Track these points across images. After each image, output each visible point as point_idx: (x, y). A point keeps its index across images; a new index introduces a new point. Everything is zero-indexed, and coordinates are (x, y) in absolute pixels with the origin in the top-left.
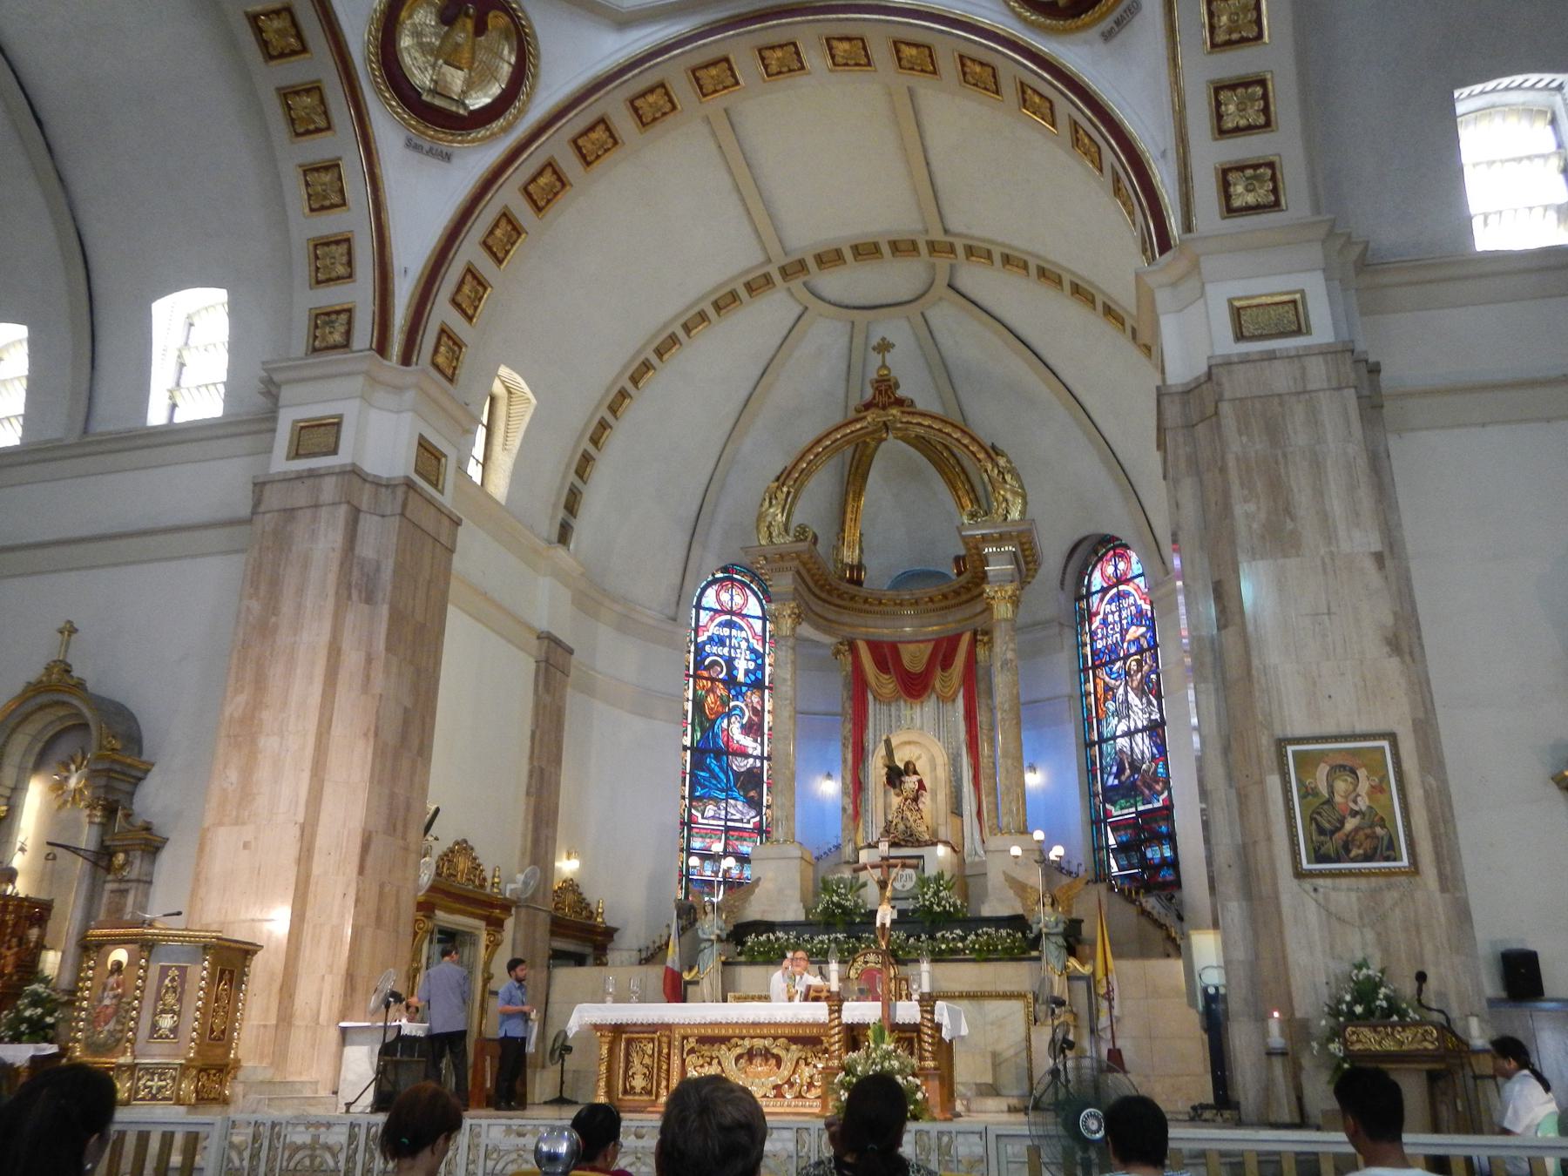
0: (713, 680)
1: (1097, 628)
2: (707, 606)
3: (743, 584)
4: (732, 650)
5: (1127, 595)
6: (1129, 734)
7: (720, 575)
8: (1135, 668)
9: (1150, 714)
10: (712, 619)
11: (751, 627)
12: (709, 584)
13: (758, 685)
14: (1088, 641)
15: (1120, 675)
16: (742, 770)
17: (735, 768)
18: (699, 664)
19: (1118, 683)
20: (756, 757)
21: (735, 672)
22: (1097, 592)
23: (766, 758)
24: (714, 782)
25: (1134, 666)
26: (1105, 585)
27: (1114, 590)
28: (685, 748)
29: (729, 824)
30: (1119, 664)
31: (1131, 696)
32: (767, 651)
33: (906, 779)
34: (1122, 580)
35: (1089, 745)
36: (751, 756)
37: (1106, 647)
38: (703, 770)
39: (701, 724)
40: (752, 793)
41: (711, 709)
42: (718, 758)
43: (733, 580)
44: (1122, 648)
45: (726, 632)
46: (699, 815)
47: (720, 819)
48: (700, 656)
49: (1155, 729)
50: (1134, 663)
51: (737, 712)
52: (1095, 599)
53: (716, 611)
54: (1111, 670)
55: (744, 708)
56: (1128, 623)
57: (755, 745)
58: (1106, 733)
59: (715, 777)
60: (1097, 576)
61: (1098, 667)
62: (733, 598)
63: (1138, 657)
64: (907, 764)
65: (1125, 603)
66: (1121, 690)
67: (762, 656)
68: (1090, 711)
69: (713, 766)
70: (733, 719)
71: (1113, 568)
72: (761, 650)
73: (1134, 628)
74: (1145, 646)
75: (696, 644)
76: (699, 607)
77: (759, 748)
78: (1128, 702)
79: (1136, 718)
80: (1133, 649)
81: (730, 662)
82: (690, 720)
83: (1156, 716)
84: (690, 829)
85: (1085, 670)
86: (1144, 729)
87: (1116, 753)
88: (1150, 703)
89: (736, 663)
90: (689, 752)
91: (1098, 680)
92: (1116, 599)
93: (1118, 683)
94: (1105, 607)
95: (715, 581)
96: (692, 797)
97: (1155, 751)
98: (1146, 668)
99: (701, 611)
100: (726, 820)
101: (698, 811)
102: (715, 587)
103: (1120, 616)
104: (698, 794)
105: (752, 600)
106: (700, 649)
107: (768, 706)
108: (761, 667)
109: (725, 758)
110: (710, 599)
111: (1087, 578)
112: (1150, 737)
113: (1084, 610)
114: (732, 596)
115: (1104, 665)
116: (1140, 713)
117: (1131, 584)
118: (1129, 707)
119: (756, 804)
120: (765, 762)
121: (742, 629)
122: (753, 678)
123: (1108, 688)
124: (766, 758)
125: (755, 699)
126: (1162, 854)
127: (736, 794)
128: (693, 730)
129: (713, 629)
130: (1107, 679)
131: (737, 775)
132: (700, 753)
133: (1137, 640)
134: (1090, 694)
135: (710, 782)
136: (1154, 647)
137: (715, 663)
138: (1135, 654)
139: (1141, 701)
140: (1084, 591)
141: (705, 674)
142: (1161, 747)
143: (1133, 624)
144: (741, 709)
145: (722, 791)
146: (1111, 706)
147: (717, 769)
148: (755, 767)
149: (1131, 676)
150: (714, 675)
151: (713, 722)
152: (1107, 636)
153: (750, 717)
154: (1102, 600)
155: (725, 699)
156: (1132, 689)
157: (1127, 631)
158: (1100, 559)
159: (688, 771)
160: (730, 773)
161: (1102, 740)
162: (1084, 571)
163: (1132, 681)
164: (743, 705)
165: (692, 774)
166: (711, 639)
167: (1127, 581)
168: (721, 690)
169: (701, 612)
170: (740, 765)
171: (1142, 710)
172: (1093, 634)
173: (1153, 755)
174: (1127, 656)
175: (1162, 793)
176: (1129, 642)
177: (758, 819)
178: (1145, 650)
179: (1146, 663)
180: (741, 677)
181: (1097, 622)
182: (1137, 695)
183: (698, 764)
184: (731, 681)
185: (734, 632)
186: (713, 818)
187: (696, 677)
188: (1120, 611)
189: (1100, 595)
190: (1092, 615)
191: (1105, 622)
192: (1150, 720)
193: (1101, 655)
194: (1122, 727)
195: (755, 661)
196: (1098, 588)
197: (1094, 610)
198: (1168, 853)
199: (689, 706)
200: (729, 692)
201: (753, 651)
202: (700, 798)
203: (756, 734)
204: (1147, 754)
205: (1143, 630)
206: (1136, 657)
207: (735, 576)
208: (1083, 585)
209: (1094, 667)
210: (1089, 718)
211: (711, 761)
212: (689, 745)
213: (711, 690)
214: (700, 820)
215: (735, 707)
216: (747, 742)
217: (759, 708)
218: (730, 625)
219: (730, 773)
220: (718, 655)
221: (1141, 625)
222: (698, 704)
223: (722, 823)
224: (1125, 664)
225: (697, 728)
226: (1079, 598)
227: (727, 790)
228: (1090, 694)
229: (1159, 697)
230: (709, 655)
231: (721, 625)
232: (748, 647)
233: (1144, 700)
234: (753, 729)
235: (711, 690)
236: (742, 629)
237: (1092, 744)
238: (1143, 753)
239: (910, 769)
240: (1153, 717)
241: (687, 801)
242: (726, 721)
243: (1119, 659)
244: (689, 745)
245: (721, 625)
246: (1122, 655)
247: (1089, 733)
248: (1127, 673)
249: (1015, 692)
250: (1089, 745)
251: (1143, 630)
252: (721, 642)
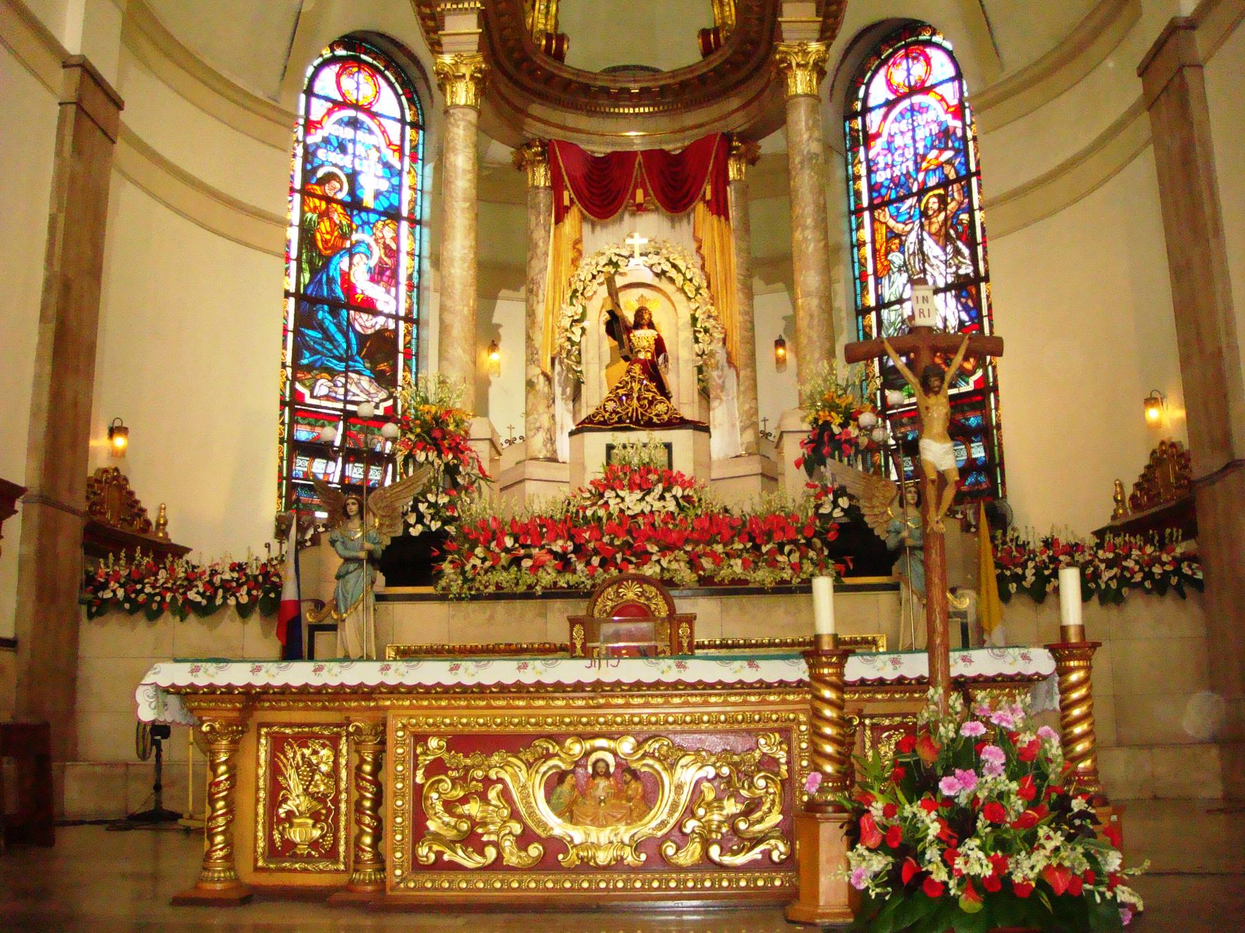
0: (329, 200)
1: (878, 154)
2: (322, 93)
3: (375, 71)
4: (357, 160)
5: (922, 110)
7: (340, 52)
8: (936, 206)
9: (958, 268)
10: (329, 113)
11: (384, 132)
12: (326, 63)
13: (392, 214)
14: (862, 169)
15: (910, 218)
16: (369, 332)
17: (358, 328)
18: (307, 175)
19: (908, 228)
20: (389, 316)
21: (359, 193)
22: (880, 106)
23: (402, 318)
24: (330, 347)
25: (934, 204)
26: (892, 97)
27: (905, 104)
28: (287, 294)
29: (350, 407)
30: (912, 201)
31: (931, 247)
32: (406, 168)
33: (638, 333)
34: (922, 88)
36: (380, 313)
37: (892, 180)
38: (313, 329)
39: (310, 262)
40: (383, 366)
41: (325, 242)
42: (334, 312)
43: (361, 64)
44: (916, 179)
45: (348, 133)
46: (306, 392)
47: (336, 400)
48: (311, 163)
49: (965, 288)
50: (935, 200)
51: (362, 248)
52: (874, 119)
53: (335, 102)
54: (898, 209)
55: (373, 244)
56: (925, 146)
57: (386, 297)
58: (889, 295)
59: (329, 337)
60: (879, 81)
61: (879, 206)
62: (360, 86)
63: (941, 191)
64: (640, 313)
65: (920, 119)
66: (912, 238)
67: (400, 174)
68: (863, 265)
69: (327, 323)
70: (356, 259)
71: (905, 74)
72: (398, 166)
73: (934, 153)
74: (952, 176)
75: (306, 147)
76: (310, 92)
77: (393, 302)
78: (923, 253)
79: (936, 274)
80: (932, 181)
81: (353, 177)
82: (294, 254)
83: (966, 269)
84: (293, 412)
85: (858, 211)
86: (948, 288)
87: (903, 322)
88: (957, 252)
89: (361, 179)
90: (292, 300)
91: (877, 225)
92: (908, 115)
93: (908, 228)
95: (333, 60)
96: (296, 366)
97: (964, 317)
98: (952, 206)
99: (314, 100)
100: (346, 402)
101: (304, 385)
102: (335, 68)
103: (913, 138)
104: (305, 362)
105: (386, 91)
106: (309, 155)
107: (406, 244)
108: (397, 189)
109: (344, 312)
110: (326, 82)
111: (863, 88)
112: (958, 297)
113: (857, 131)
114: (358, 83)
115: (890, 202)
116: (943, 266)
117: (932, 94)
118: (924, 258)
119: (386, 380)
120: (401, 323)
121: (370, 132)
122: (386, 204)
123: (892, 235)
124: (402, 318)
125: (388, 233)
126: (969, 454)
127: (360, 366)
128: (300, 270)
129: (330, 128)
130: (891, 223)
131: (362, 338)
132: (306, 302)
133: (940, 166)
134: (864, 244)
135: (324, 347)
137: (330, 177)
138: (936, 187)
139: (944, 249)
140: (858, 106)
141: (318, 190)
142: (975, 310)
143: (933, 147)
144: (369, 246)
145: (340, 359)
146: (896, 258)
147: (333, 329)
148: (387, 330)
149: (928, 217)
150: (331, 194)
151: (328, 261)
152: (893, 166)
153: (380, 258)
154: (885, 118)
155: (346, 229)
156: (930, 234)
157: (924, 157)
158: (884, 62)
159: (291, 326)
160: (352, 335)
161: (881, 305)
162: (857, 78)
163: (930, 224)
164: (371, 241)
165: (297, 332)
166: (326, 141)
168: (338, 215)
169: (314, 100)
170: (365, 323)
171: (946, 262)
173: (961, 323)
174: (923, 191)
175: (973, 373)
176: (927, 171)
177: (390, 402)
178: (954, 182)
179: (953, 199)
180: (369, 202)
181: (878, 145)
182: (937, 243)
183: (305, 318)
184: (354, 205)
185: (361, 135)
186: (327, 397)
187: (306, 193)
188: (913, 130)
189: (883, 110)
190: (869, 139)
191: (889, 149)
192: (957, 276)
193: (883, 191)
195: (389, 179)
196: (882, 101)
197: (873, 131)
198: (978, 452)
199: (293, 234)
200: (352, 222)
201: (387, 165)
202: (309, 368)
203: (389, 284)
204: (953, 323)
205: (949, 154)
206: (936, 192)
207: (363, 57)
208: (857, 99)
209: (872, 208)
210: (863, 277)
211: (323, 314)
212: (292, 289)
213: (325, 214)
214: (308, 400)
215: (358, 243)
216: (375, 292)
217: (394, 246)
218: (354, 124)
219: (352, 335)
220: (335, 165)
221: (946, 148)
222: (307, 233)
223: (340, 405)
224: (919, 201)
225: (305, 266)
226: (852, 116)
227: (346, 359)
228: (864, 244)
229: (972, 245)
230: (322, 165)
231: (340, 122)
232: (380, 158)
233: (949, 249)
234: (384, 274)
235: (325, 214)
236: (370, 132)
237: (866, 311)
238: (945, 320)
239: (642, 319)
240: (962, 272)
241: (289, 370)
242: (346, 259)
243: (911, 195)
244: (292, 289)
245: (340, 122)
246: (915, 189)
247: (863, 296)
248: (924, 214)
249: (822, 202)
250: (864, 311)
251: (949, 154)
252: (342, 148)
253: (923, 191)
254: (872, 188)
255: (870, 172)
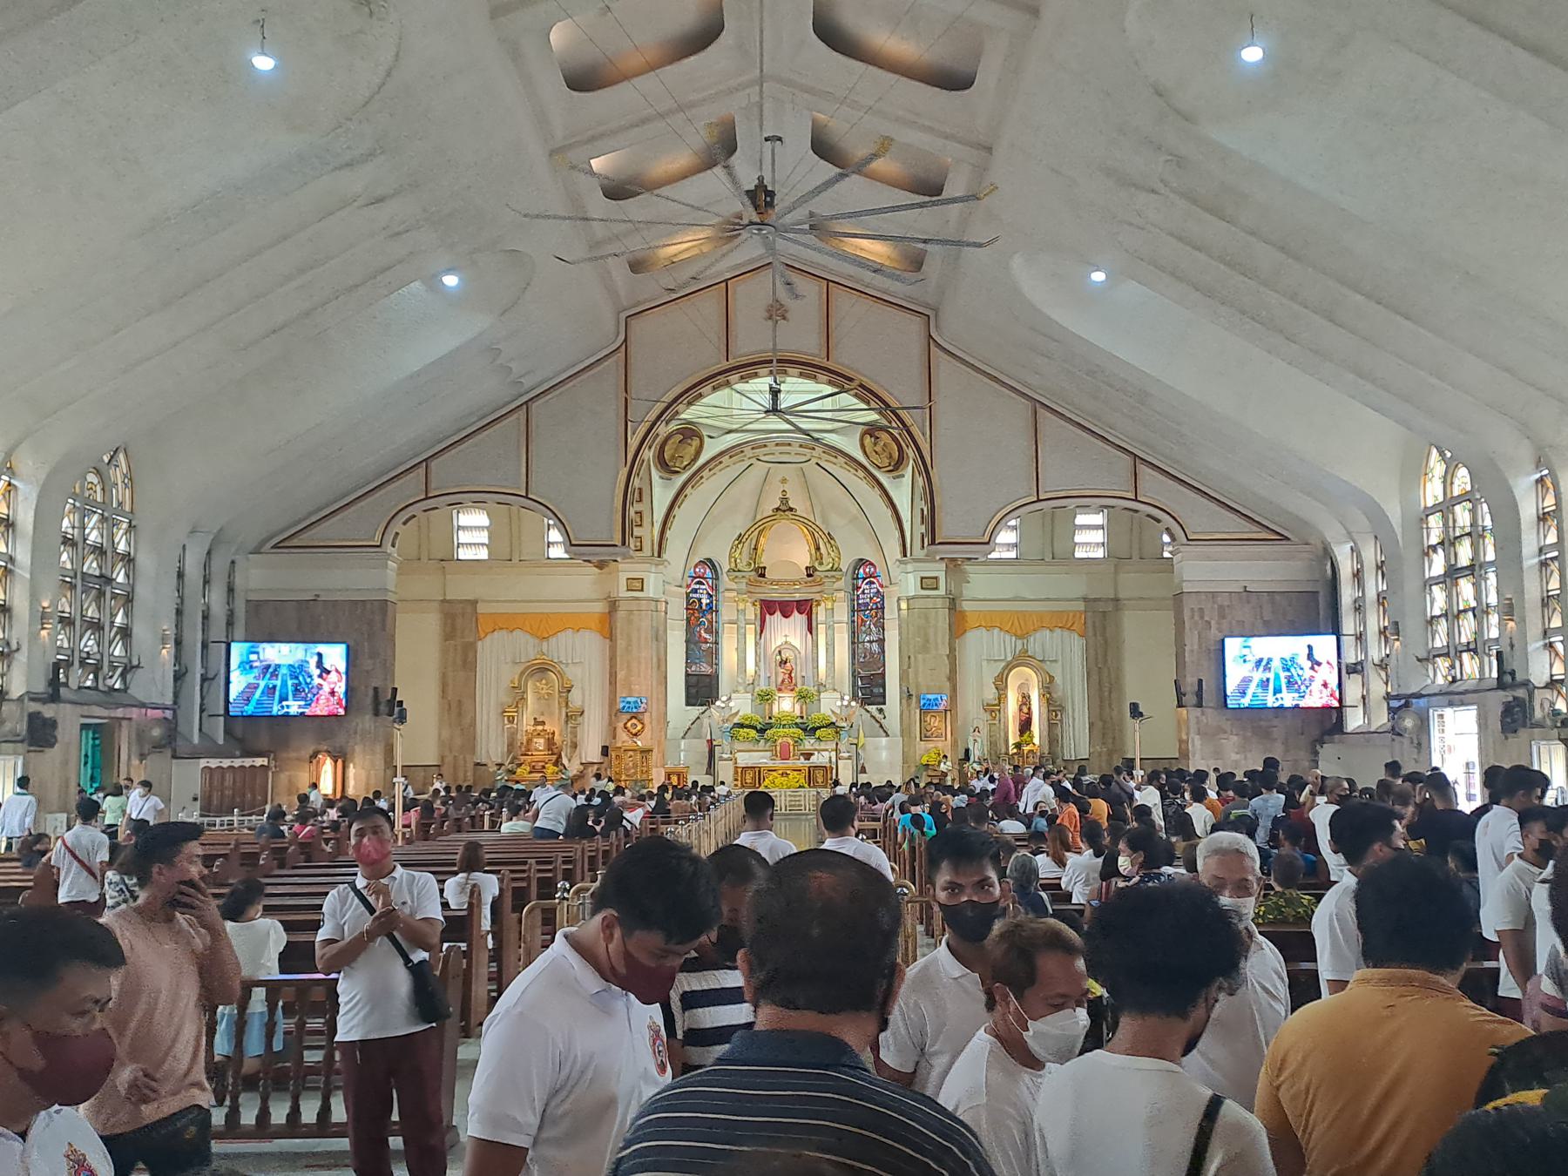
5: (874, 583)
6: (870, 642)
35: (853, 643)
52: (860, 581)
60: (861, 571)
94: (864, 586)
136: (883, 608)
146: (863, 628)
167: (874, 577)
172: (858, 596)
174: (872, 609)
190: (859, 588)
191: (863, 593)
194: (868, 638)
229: (883, 630)
253: (872, 609)
254: (858, 604)
255: (858, 599)
